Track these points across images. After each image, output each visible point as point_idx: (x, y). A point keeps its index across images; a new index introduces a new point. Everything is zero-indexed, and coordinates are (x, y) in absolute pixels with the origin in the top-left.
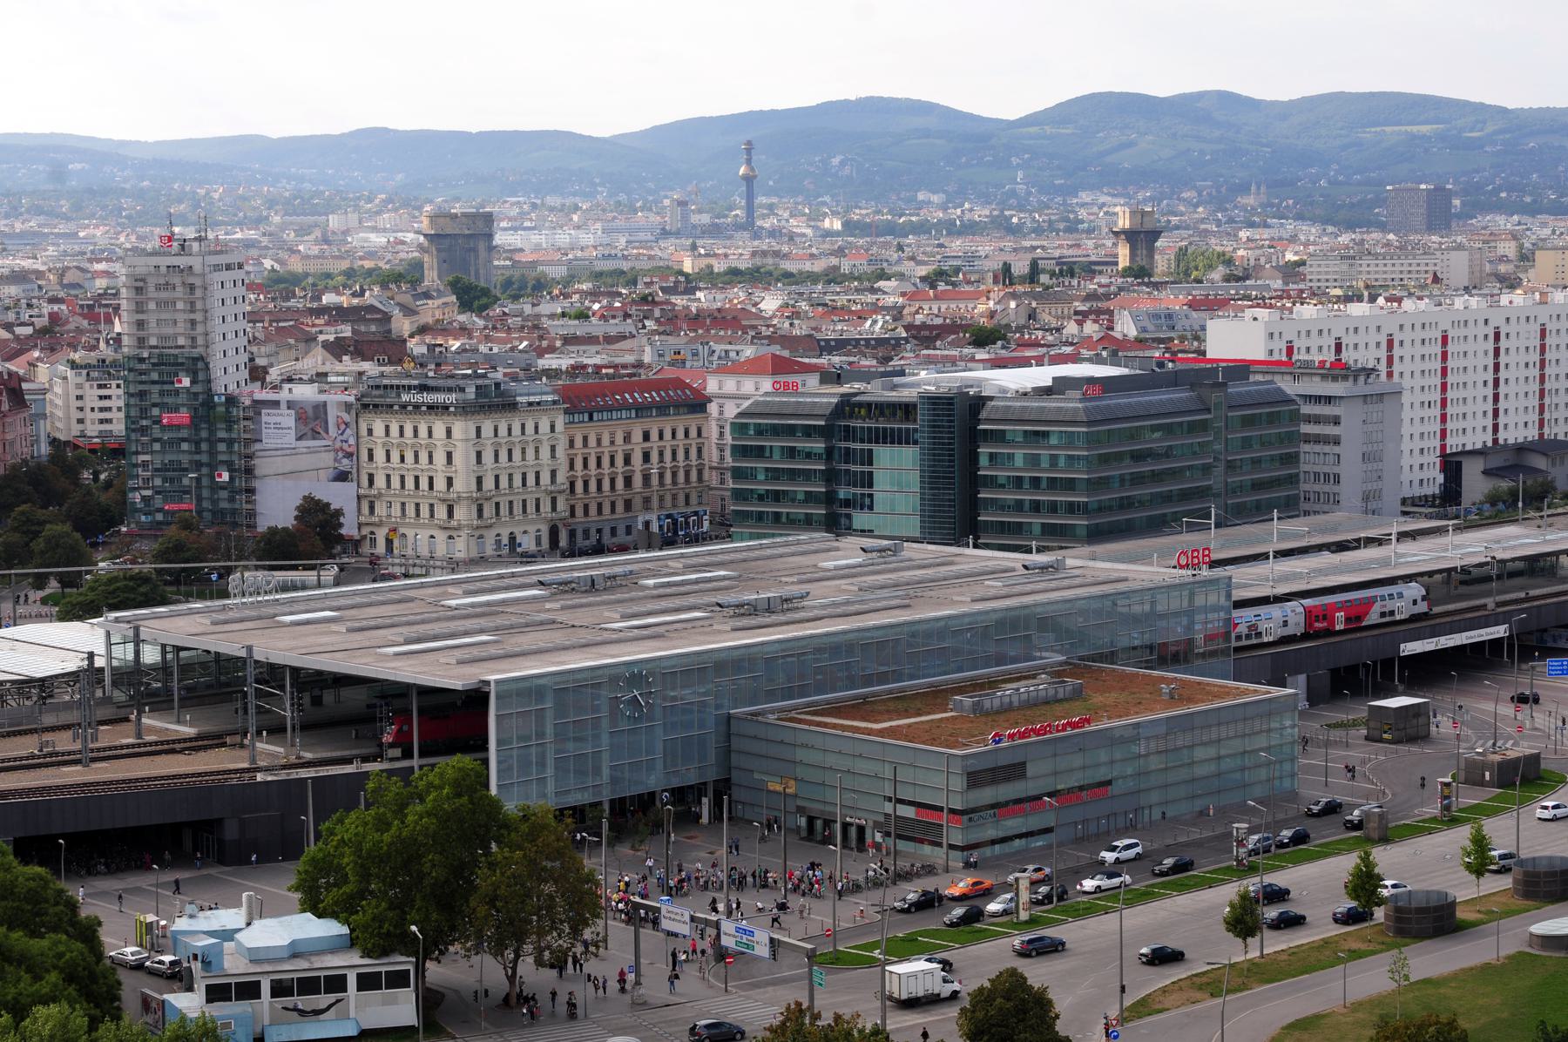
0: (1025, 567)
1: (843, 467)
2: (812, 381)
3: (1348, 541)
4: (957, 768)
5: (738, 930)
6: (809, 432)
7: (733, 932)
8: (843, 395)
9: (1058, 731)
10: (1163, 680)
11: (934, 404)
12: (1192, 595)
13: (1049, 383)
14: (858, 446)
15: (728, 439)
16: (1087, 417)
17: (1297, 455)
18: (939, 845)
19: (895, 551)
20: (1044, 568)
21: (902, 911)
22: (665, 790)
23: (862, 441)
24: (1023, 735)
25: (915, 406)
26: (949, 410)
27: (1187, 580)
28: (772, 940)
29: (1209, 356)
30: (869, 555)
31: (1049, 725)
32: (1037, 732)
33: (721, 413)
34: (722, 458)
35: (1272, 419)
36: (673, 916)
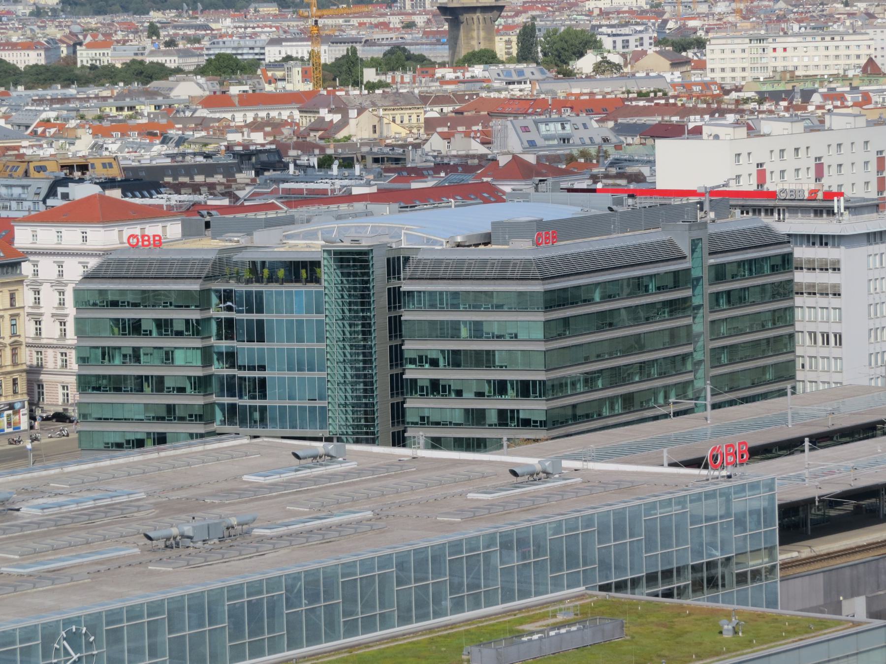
0: (514, 473)
1: (224, 345)
2: (174, 229)
6: (184, 300)
8: (221, 251)
10: (728, 615)
11: (341, 260)
12: (728, 501)
13: (488, 229)
14: (245, 316)
15: (71, 310)
16: (541, 271)
17: (791, 309)
23: (250, 311)
25: (316, 264)
26: (362, 267)
29: (660, 186)
30: (302, 462)
33: (36, 273)
34: (64, 333)
35: (753, 266)
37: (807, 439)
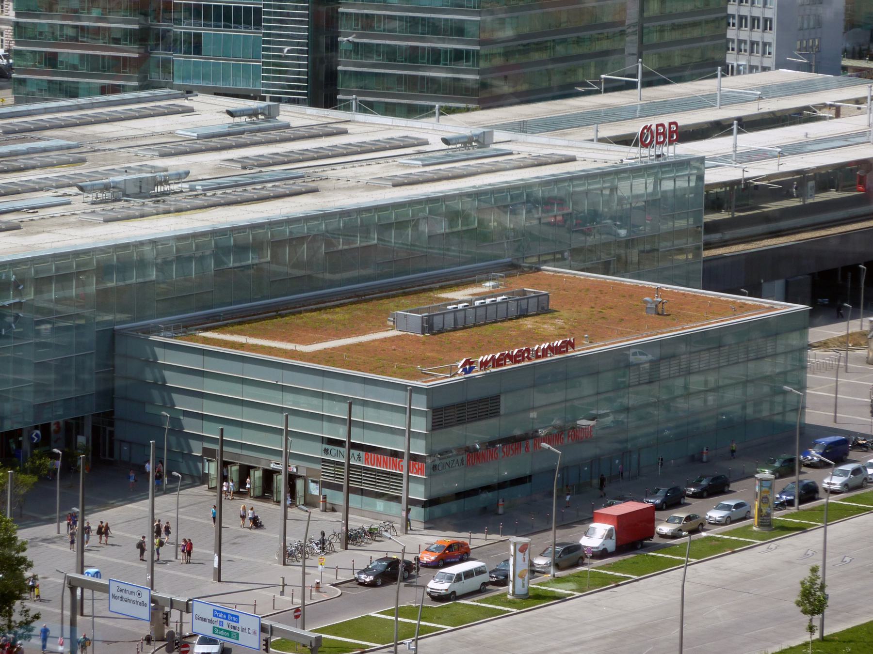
3: (807, 108)
4: (421, 404)
5: (216, 613)
7: (210, 616)
9: (538, 357)
18: (397, 499)
19: (270, 114)
20: (467, 142)
21: (372, 585)
22: (36, 428)
24: (497, 363)
27: (650, 163)
28: (263, 629)
31: (528, 350)
32: (514, 359)
36: (126, 596)
37: (735, 122)
